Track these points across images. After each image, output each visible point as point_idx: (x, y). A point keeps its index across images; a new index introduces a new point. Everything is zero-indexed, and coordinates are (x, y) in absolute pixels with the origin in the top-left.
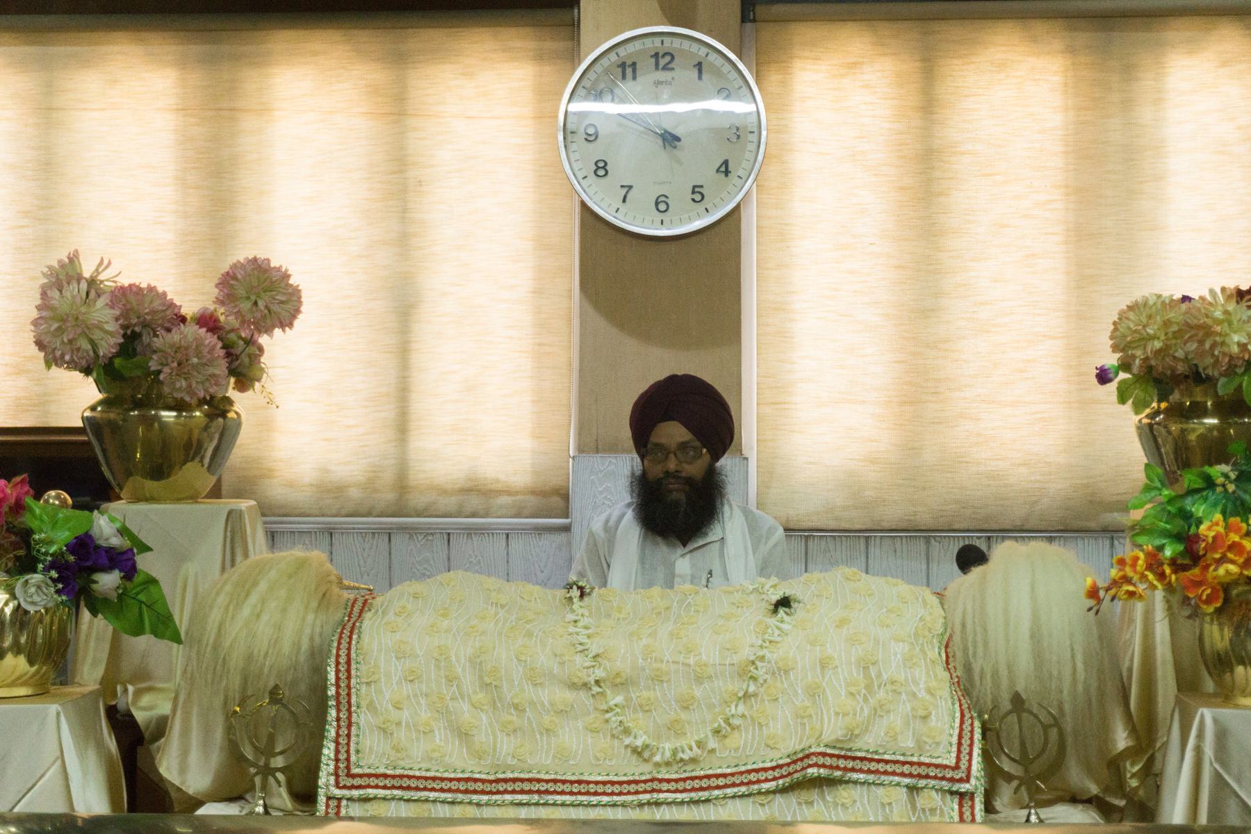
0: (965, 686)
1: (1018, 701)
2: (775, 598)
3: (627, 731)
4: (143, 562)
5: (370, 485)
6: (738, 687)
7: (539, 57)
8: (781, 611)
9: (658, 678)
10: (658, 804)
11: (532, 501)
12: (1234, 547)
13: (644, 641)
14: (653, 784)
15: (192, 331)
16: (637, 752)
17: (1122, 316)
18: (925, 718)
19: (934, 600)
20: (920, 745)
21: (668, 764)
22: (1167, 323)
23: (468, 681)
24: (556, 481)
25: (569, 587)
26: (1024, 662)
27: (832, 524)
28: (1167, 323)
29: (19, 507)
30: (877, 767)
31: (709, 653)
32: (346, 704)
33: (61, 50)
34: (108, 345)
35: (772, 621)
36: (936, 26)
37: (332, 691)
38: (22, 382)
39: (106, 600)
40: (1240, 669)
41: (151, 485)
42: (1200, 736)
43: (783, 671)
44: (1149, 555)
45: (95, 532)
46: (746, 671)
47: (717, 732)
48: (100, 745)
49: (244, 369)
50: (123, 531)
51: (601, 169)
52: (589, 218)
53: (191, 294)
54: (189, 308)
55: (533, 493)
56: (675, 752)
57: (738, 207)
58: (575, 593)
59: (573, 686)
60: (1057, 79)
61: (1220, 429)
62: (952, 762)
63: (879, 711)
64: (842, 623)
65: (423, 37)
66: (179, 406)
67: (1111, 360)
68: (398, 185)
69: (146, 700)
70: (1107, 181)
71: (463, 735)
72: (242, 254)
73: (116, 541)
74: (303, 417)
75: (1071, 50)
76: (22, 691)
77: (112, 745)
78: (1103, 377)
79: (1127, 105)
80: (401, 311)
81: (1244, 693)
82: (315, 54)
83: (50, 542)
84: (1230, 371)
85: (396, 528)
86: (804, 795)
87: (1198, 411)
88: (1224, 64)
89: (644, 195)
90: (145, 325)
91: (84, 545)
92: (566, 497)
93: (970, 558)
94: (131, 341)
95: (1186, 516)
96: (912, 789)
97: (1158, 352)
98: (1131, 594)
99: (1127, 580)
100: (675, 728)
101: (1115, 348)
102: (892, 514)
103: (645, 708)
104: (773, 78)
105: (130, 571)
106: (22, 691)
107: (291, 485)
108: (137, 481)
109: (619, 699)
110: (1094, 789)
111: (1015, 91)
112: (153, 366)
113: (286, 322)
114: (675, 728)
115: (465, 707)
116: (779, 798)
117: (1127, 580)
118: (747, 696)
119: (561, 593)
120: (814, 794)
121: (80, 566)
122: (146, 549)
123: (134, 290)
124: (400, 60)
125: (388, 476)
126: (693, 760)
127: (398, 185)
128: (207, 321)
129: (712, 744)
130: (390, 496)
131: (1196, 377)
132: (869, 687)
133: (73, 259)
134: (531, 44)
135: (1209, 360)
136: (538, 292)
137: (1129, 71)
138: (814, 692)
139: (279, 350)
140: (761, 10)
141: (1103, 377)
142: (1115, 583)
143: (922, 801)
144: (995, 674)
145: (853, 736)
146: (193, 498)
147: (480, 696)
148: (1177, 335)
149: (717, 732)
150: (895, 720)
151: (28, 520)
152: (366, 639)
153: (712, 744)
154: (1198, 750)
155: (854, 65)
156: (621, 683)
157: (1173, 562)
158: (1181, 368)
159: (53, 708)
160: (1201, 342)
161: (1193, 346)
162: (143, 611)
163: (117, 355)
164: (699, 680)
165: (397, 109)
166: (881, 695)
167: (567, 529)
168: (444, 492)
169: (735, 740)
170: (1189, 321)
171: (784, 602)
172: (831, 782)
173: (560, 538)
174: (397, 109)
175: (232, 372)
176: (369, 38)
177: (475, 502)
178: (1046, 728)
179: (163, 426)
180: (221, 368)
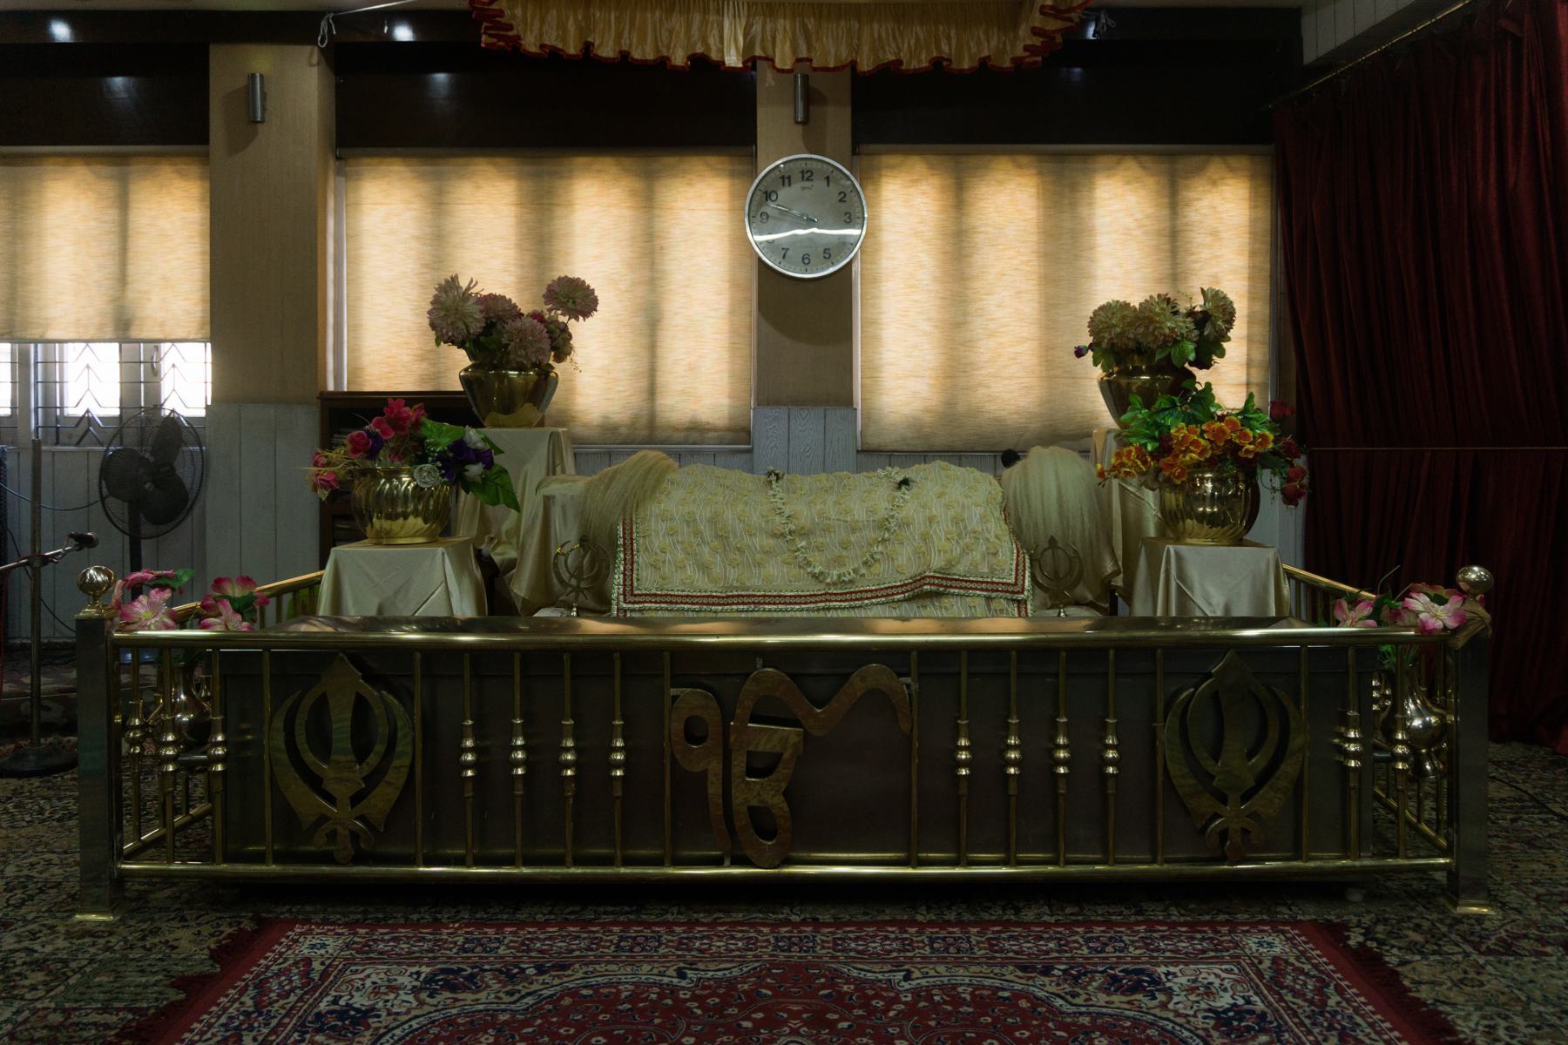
0: (1017, 533)
1: (1052, 541)
2: (899, 478)
3: (809, 564)
4: (497, 459)
5: (633, 424)
6: (878, 535)
8: (903, 488)
9: (827, 530)
10: (829, 609)
12: (1195, 443)
14: (827, 597)
15: (528, 322)
16: (815, 577)
17: (1095, 313)
18: (995, 554)
19: (995, 482)
20: (992, 571)
21: (835, 584)
22: (1124, 317)
23: (708, 534)
25: (769, 474)
26: (1054, 517)
27: (905, 448)
28: (1124, 317)
29: (418, 424)
30: (966, 585)
31: (859, 513)
32: (629, 548)
34: (476, 327)
35: (899, 494)
36: (963, 158)
37: (621, 542)
39: (474, 483)
40: (1189, 521)
41: (502, 418)
42: (1168, 562)
43: (905, 524)
44: (1138, 450)
45: (467, 439)
46: (883, 525)
47: (865, 563)
48: (471, 575)
49: (561, 344)
50: (486, 440)
53: (525, 301)
54: (525, 309)
55: (729, 429)
56: (839, 576)
57: (850, 263)
58: (773, 478)
59: (774, 536)
60: (1033, 190)
62: (1012, 581)
63: (967, 550)
64: (940, 495)
66: (520, 368)
67: (1087, 340)
68: (649, 252)
69: (499, 550)
70: (1063, 247)
71: (704, 568)
73: (480, 445)
74: (595, 376)
75: (1040, 174)
77: (478, 574)
78: (1079, 353)
79: (1074, 205)
80: (650, 324)
81: (1190, 536)
83: (437, 445)
84: (1164, 346)
85: (652, 444)
86: (921, 602)
87: (1138, 371)
88: (1128, 183)
90: (499, 318)
91: (459, 446)
92: (749, 432)
93: (1010, 457)
94: (490, 327)
95: (1158, 426)
96: (988, 599)
97: (1118, 335)
98: (1127, 473)
99: (1123, 465)
100: (838, 561)
101: (1092, 333)
102: (940, 441)
103: (819, 549)
104: (870, 188)
105: (489, 464)
107: (585, 426)
108: (493, 414)
110: (1090, 597)
111: (1009, 199)
112: (504, 341)
113: (586, 314)
114: (838, 561)
115: (706, 550)
116: (905, 605)
117: (1123, 465)
118: (884, 540)
119: (763, 478)
120: (928, 602)
121: (459, 456)
122: (500, 452)
123: (492, 297)
124: (650, 178)
125: (644, 421)
126: (851, 581)
127: (649, 252)
128: (537, 316)
129: (863, 571)
130: (645, 432)
131: (1140, 350)
132: (959, 535)
133: (454, 279)
135: (1151, 339)
136: (732, 312)
137: (1074, 188)
138: (925, 538)
139: (583, 332)
140: (864, 148)
141: (1079, 353)
142: (1114, 468)
143: (994, 605)
144: (1036, 524)
145: (950, 564)
146: (529, 425)
148: (1130, 324)
149: (865, 563)
150: (976, 555)
151: (424, 432)
153: (863, 571)
155: (917, 181)
156: (804, 533)
157: (1151, 454)
158: (1131, 345)
159: (440, 550)
160: (1147, 327)
161: (1141, 330)
162: (499, 489)
163: (481, 334)
164: (854, 530)
165: (648, 203)
166: (967, 540)
167: (750, 451)
168: (675, 429)
169: (877, 568)
170: (1143, 317)
171: (905, 482)
173: (745, 457)
175: (553, 348)
177: (695, 436)
178: (1070, 559)
179: (510, 380)
180: (546, 344)
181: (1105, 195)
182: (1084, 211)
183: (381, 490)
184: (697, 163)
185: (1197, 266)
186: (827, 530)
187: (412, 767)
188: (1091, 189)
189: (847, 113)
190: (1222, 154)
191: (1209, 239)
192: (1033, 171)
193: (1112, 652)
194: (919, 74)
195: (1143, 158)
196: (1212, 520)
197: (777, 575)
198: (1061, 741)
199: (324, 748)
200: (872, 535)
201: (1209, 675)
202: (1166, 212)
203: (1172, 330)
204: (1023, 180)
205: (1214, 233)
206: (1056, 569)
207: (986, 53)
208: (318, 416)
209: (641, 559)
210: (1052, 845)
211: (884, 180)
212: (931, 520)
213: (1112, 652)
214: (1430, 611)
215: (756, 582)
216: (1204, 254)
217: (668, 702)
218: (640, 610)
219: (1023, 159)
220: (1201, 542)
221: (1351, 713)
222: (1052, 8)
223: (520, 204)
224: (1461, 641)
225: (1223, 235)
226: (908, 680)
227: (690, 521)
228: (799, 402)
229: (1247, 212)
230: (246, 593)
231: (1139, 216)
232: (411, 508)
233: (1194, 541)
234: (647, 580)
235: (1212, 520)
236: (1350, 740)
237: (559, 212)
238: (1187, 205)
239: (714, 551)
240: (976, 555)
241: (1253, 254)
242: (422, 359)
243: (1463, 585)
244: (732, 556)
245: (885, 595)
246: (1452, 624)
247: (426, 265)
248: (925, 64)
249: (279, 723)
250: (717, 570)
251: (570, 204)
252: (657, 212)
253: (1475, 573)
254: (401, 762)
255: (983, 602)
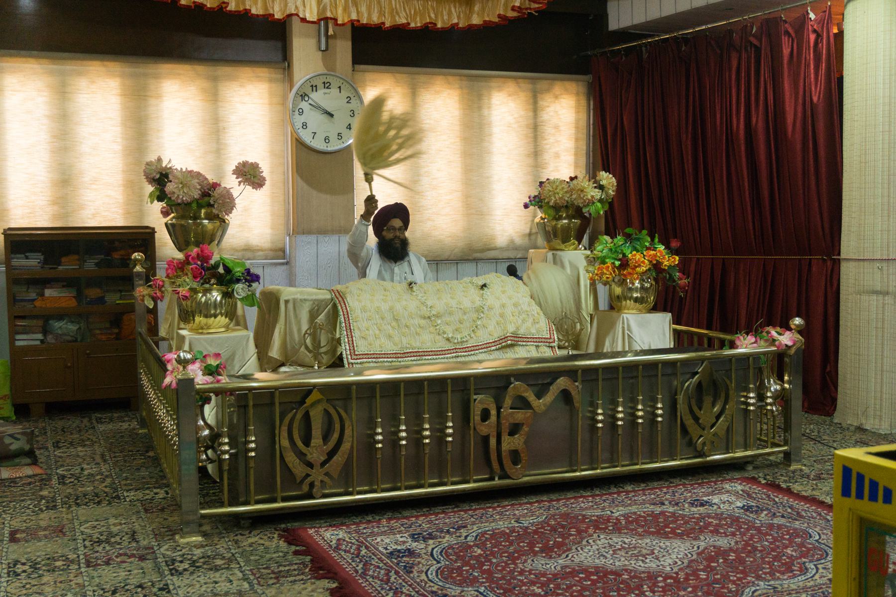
2: (481, 283)
3: (444, 333)
7: (271, 80)
11: (271, 254)
13: (445, 301)
16: (448, 339)
20: (538, 331)
24: (280, 245)
31: (467, 304)
33: (70, 66)
36: (417, 76)
38: (56, 208)
42: (623, 323)
51: (304, 126)
52: (300, 145)
55: (271, 250)
59: (424, 318)
60: (457, 98)
61: (569, 224)
63: (524, 321)
65: (224, 70)
71: (390, 337)
72: (152, 158)
75: (461, 88)
76: (223, 330)
79: (480, 108)
82: (179, 74)
86: (505, 350)
88: (510, 95)
89: (320, 136)
94: (206, 194)
96: (537, 346)
106: (223, 330)
109: (439, 322)
120: (508, 350)
124: (215, 79)
133: (159, 160)
134: (267, 75)
137: (480, 97)
138: (502, 315)
140: (357, 66)
147: (394, 324)
150: (529, 324)
152: (351, 304)
154: (623, 328)
156: (438, 316)
164: (465, 313)
165: (214, 98)
169: (480, 333)
171: (484, 286)
172: (512, 346)
173: (285, 267)
174: (214, 98)
176: (201, 68)
177: (249, 254)
179: (204, 226)
181: (498, 102)
182: (485, 112)
183: (200, 302)
184: (246, 72)
185: (548, 147)
186: (451, 314)
187: (352, 447)
188: (489, 99)
189: (349, 44)
190: (562, 80)
191: (553, 131)
192: (457, 86)
193: (660, 365)
194: (415, 31)
195: (520, 80)
196: (636, 300)
197: (427, 340)
198: (620, 409)
199: (307, 442)
200: (475, 316)
201: (697, 373)
202: (531, 114)
203: (592, 197)
204: (451, 92)
205: (556, 127)
206: (567, 329)
207: (455, 21)
208: (157, 254)
209: (356, 334)
210: (613, 462)
211: (368, 88)
212: (503, 306)
213: (660, 365)
214: (786, 339)
215: (418, 344)
216: (551, 140)
217: (472, 401)
218: (361, 363)
219: (451, 78)
220: (634, 311)
221: (751, 386)
222: (519, 7)
223: (123, 95)
224: (792, 351)
225: (562, 128)
226: (577, 384)
227: (378, 311)
228: (323, 232)
229: (574, 115)
230: (218, 362)
231: (516, 116)
232: (218, 311)
233: (631, 311)
234: (362, 347)
235: (636, 300)
236: (750, 398)
237: (152, 101)
238: (542, 110)
239: (393, 328)
240: (529, 324)
241: (577, 140)
242: (54, 203)
243: (793, 327)
244: (404, 330)
245: (486, 347)
246: (790, 343)
247: (54, 137)
248: (419, 25)
249: (285, 428)
250: (396, 339)
251: (159, 97)
252: (220, 104)
253: (798, 321)
254: (346, 446)
255: (534, 348)
